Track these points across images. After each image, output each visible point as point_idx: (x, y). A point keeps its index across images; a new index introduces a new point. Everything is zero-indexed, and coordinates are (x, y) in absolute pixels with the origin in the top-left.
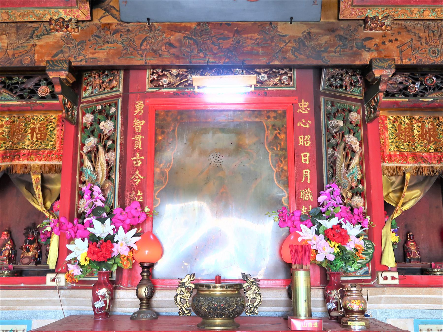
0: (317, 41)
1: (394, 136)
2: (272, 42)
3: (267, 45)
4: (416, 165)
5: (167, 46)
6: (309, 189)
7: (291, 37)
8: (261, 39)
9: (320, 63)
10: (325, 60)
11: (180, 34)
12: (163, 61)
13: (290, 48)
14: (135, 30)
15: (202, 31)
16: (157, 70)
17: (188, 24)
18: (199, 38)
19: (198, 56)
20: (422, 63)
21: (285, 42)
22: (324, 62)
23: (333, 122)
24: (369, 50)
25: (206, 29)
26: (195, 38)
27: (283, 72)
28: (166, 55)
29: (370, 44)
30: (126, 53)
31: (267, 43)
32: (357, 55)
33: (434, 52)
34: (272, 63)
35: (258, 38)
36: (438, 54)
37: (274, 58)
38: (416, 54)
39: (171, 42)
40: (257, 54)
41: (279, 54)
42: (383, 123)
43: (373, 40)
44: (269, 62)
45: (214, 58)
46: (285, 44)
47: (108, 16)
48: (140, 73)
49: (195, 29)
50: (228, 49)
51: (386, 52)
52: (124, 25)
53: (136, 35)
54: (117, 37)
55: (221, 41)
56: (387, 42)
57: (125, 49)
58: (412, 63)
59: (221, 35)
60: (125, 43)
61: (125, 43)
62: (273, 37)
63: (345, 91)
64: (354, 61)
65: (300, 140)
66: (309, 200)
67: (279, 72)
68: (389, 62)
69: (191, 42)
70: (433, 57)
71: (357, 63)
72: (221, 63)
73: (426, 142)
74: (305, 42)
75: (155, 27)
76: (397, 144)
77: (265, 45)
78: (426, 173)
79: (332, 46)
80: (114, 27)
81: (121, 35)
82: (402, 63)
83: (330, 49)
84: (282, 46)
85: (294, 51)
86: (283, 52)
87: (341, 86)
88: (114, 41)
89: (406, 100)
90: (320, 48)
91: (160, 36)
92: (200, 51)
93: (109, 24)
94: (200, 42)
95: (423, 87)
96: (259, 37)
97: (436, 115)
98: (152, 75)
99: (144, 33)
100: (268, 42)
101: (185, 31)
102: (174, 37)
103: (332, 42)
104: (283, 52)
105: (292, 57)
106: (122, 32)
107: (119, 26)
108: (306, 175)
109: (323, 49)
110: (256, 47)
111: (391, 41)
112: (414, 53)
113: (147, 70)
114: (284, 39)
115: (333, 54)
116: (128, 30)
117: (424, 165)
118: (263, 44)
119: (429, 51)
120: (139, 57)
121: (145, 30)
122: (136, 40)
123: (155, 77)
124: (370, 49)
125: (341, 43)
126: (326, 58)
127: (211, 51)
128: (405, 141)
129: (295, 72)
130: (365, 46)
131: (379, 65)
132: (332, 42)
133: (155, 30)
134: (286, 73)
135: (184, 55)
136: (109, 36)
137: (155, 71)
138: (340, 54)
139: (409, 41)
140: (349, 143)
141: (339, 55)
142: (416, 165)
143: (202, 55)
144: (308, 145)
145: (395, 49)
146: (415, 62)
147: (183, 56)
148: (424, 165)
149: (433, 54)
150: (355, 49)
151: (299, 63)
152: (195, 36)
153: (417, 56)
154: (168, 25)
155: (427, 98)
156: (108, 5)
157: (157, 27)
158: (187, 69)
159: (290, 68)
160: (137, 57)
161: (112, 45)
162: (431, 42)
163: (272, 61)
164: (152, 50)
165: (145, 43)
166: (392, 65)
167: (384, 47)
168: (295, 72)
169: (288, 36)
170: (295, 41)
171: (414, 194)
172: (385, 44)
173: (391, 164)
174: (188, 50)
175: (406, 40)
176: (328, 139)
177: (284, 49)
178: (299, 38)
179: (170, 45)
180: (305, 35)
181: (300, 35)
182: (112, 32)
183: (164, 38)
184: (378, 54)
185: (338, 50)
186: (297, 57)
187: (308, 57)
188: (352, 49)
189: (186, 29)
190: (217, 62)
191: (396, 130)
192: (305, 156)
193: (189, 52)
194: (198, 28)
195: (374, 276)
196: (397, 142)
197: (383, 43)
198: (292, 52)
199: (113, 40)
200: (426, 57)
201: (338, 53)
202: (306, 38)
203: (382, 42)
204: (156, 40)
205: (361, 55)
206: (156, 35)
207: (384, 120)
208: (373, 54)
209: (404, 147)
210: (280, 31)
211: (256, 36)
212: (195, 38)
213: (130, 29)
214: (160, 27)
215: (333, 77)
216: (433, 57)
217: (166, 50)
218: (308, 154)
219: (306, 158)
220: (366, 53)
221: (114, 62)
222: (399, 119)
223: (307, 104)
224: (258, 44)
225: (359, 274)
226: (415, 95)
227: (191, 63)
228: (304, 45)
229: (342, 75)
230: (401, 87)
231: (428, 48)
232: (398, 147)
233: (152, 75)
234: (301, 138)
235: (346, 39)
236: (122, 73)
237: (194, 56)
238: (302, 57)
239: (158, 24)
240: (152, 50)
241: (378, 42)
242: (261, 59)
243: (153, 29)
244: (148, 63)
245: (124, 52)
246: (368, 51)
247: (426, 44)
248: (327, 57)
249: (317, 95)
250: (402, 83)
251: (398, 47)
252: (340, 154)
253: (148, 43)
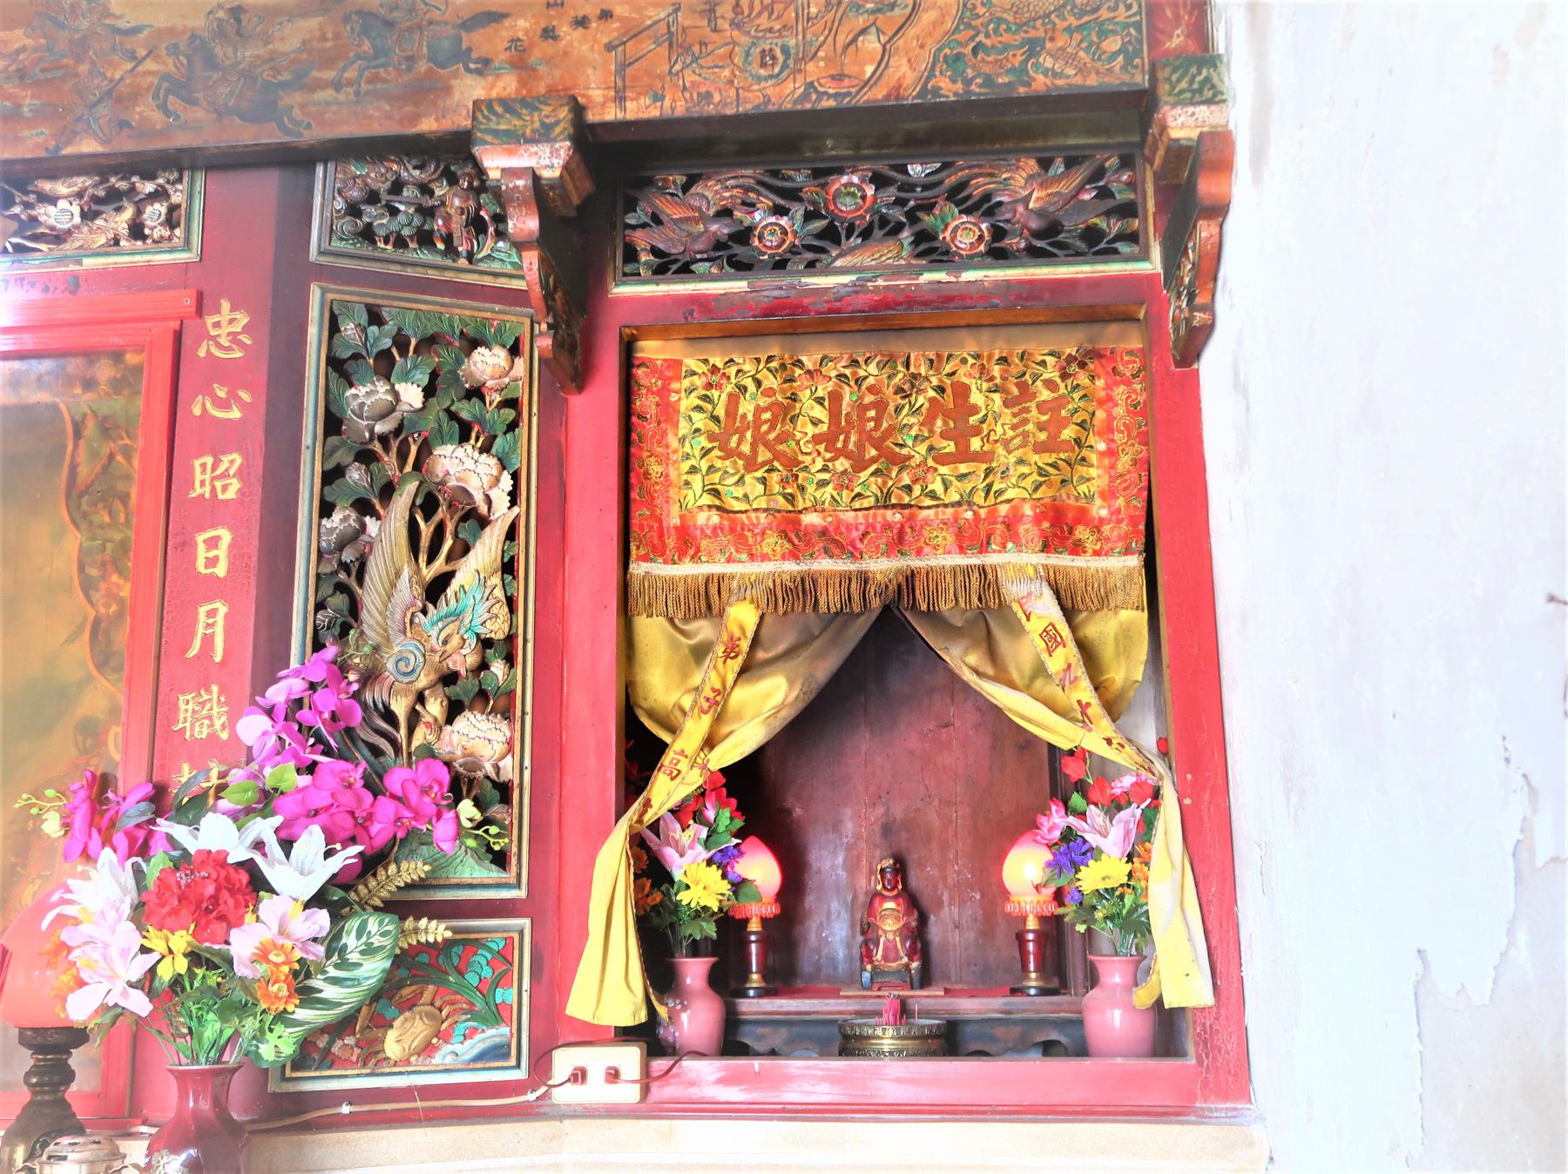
0: (267, 43)
1: (703, 441)
2: (79, 60)
3: (59, 73)
4: (791, 567)
6: (215, 688)
7: (160, 33)
8: (35, 50)
13: (149, 79)
20: (711, 110)
21: (132, 56)
22: (286, 131)
23: (366, 394)
24: (484, 66)
27: (149, 187)
29: (481, 41)
31: (63, 67)
32: (429, 91)
33: (766, 58)
34: (68, 151)
35: (24, 49)
36: (785, 66)
37: (79, 127)
38: (687, 72)
41: (103, 110)
42: (664, 392)
43: (507, 23)
44: (58, 149)
46: (129, 66)
51: (557, 73)
56: (564, 30)
58: (668, 113)
62: (85, 37)
63: (449, 262)
64: (416, 118)
65: (198, 477)
66: (213, 737)
67: (133, 189)
68: (546, 110)
70: (759, 79)
71: (428, 125)
73: (842, 464)
74: (218, 50)
76: (716, 477)
77: (49, 75)
78: (829, 599)
79: (327, 61)
82: (620, 116)
83: (315, 73)
84: (117, 76)
85: (168, 92)
86: (119, 100)
87: (425, 239)
89: (739, 286)
90: (276, 71)
95: (819, 225)
96: (29, 42)
97: (899, 346)
100: (65, 61)
103: (329, 44)
104: (119, 100)
105: (157, 117)
108: (208, 626)
109: (286, 76)
111: (582, 22)
112: (677, 67)
114: (130, 42)
117: (825, 565)
118: (43, 70)
119: (748, 54)
124: (486, 62)
125: (367, 46)
126: (296, 112)
128: (751, 465)
129: (199, 185)
130: (469, 50)
131: (503, 127)
132: (329, 44)
134: (160, 195)
138: (357, 93)
139: (663, 15)
140: (452, 483)
141: (352, 97)
142: (791, 567)
144: (231, 494)
145: (597, 56)
146: (680, 110)
148: (825, 565)
149: (763, 65)
150: (423, 66)
151: (183, 140)
153: (690, 78)
155: (829, 271)
162: (759, 14)
163: (68, 143)
166: (557, 123)
167: (550, 52)
168: (199, 185)
169: (146, 32)
170: (174, 50)
171: (768, 695)
172: (555, 38)
173: (686, 569)
175: (651, 12)
176: (330, 465)
178: (194, 37)
180: (219, 19)
181: (198, 22)
184: (522, 83)
185: (351, 74)
186: (178, 117)
188: (409, 69)
191: (716, 419)
192: (213, 543)
195: (541, 1066)
196: (711, 469)
197: (549, 34)
198: (156, 97)
200: (731, 82)
201: (350, 90)
202: (220, 33)
203: (545, 30)
205: (448, 90)
207: (671, 379)
208: (501, 84)
209: (750, 494)
210: (118, 12)
215: (373, 198)
216: (759, 79)
218: (226, 536)
219: (215, 552)
220: (470, 80)
222: (732, 370)
223: (243, 319)
224: (22, 74)
225: (449, 1060)
226: (780, 265)
228: (211, 62)
229: (426, 189)
230: (721, 229)
231: (745, 40)
232: (716, 493)
234: (204, 466)
235: (389, 24)
238: (198, 113)
241: (527, 31)
242: (26, 133)
246: (479, 72)
247: (735, 25)
248: (302, 107)
249: (292, 273)
250: (725, 213)
251: (609, 47)
252: (388, 530)
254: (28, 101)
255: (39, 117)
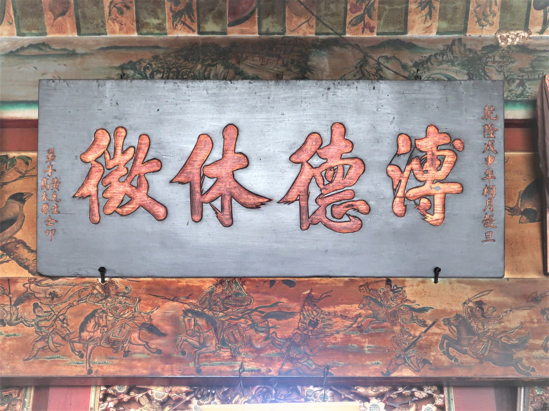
0: (500, 322)
2: (394, 324)
3: (383, 330)
5: (144, 331)
7: (438, 313)
8: (367, 317)
9: (511, 374)
10: (523, 366)
11: (175, 303)
12: (131, 368)
13: (436, 337)
14: (70, 293)
15: (228, 297)
16: (116, 388)
17: (196, 282)
18: (221, 314)
19: (217, 356)
21: (424, 324)
25: (237, 294)
26: (210, 313)
27: (423, 395)
28: (139, 352)
30: (43, 348)
31: (382, 327)
34: (395, 375)
35: (360, 315)
37: (399, 361)
39: (154, 322)
40: (360, 352)
41: (411, 352)
45: (255, 360)
46: (424, 329)
47: (8, 261)
48: (75, 395)
49: (211, 293)
50: (289, 339)
52: (44, 282)
53: (71, 305)
54: (26, 311)
55: (272, 321)
57: (43, 338)
59: (272, 306)
60: (43, 323)
61: (43, 323)
62: (395, 311)
67: (412, 395)
69: (201, 322)
72: (273, 373)
74: (473, 324)
75: (117, 287)
77: (377, 331)
79: (538, 335)
80: (19, 287)
81: (36, 306)
84: (417, 334)
85: (448, 345)
86: (421, 347)
88: (17, 319)
90: (509, 338)
91: (128, 307)
92: (223, 343)
93: (9, 281)
94: (223, 322)
96: (363, 312)
98: (104, 400)
99: (91, 300)
100: (385, 324)
101: (188, 298)
102: (162, 312)
103: (536, 325)
104: (421, 347)
105: (444, 358)
106: (38, 298)
107: (33, 285)
109: (515, 341)
110: (355, 336)
113: (93, 389)
114: (421, 316)
115: (540, 353)
116: (54, 295)
118: (373, 328)
120: (76, 358)
121: (92, 294)
122: (69, 317)
123: (111, 405)
126: (524, 361)
127: (249, 343)
132: (536, 325)
133: (117, 294)
134: (430, 398)
135: (184, 353)
136: (7, 308)
137: (110, 391)
143: (226, 354)
147: (180, 356)
151: (461, 373)
152: (210, 309)
154: (148, 283)
156: (11, 237)
157: (121, 287)
158: (190, 386)
159: (440, 385)
160: (70, 357)
161: (12, 328)
163: (394, 370)
164: (108, 340)
165: (91, 325)
169: (430, 311)
170: (448, 322)
174: (194, 341)
177: (421, 341)
178: (458, 316)
179: (152, 329)
180: (470, 307)
181: (459, 308)
182: (14, 299)
183: (136, 314)
186: (456, 360)
187: (482, 359)
189: (190, 292)
190: (263, 370)
193: (194, 347)
194: (219, 290)
198: (442, 347)
199: (14, 317)
202: (472, 314)
204: (116, 317)
206: (118, 305)
210: (412, 299)
211: (355, 309)
212: (210, 313)
213: (57, 290)
214: (130, 287)
217: (140, 342)
221: (14, 368)
224: (360, 329)
227: (199, 371)
228: (470, 331)
233: (104, 400)
236: (31, 393)
237: (206, 357)
238: (467, 359)
239: (125, 280)
240: (108, 340)
242: (368, 363)
243: (113, 293)
244: (97, 371)
245: (39, 345)
248: (528, 359)
253: (97, 324)
254: (367, 345)
255: (375, 354)
